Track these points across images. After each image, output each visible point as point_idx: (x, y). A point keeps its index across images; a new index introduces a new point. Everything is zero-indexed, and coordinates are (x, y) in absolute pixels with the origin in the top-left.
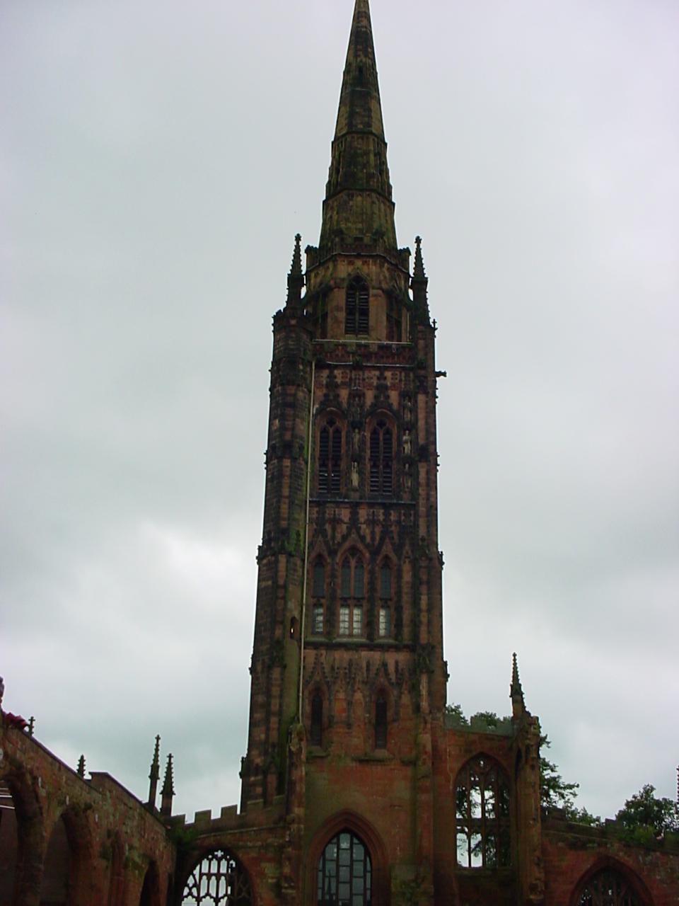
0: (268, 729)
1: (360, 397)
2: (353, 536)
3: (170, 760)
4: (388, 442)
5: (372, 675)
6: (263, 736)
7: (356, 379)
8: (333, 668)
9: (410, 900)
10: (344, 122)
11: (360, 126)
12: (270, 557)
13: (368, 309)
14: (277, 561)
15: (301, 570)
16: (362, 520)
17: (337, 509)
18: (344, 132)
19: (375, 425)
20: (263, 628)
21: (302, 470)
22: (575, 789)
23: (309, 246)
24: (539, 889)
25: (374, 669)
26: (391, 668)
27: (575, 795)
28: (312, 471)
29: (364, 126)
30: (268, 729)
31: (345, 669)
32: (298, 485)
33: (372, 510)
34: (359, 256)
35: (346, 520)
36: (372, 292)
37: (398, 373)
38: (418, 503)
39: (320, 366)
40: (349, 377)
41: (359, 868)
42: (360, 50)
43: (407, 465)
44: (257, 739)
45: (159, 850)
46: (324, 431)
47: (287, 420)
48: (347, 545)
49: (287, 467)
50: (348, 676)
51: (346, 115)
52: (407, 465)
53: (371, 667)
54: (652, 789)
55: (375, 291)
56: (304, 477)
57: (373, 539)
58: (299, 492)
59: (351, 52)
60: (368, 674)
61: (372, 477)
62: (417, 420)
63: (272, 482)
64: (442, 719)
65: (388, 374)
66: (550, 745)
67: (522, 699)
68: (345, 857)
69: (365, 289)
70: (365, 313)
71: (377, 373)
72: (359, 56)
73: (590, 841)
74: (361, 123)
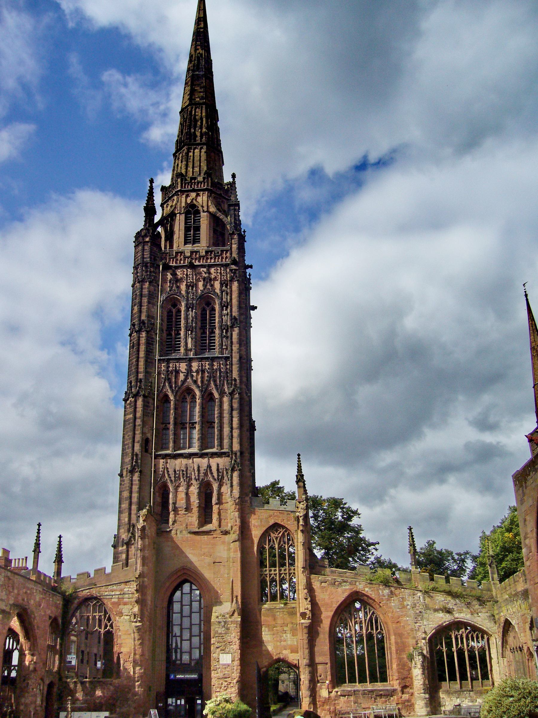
0: (130, 514)
1: (193, 287)
2: (188, 380)
3: (60, 539)
4: (212, 316)
5: (202, 474)
6: (127, 519)
7: (190, 274)
8: (175, 471)
9: (224, 626)
10: (187, 97)
11: (198, 99)
12: (131, 398)
13: (200, 226)
14: (136, 401)
15: (152, 406)
16: (194, 369)
17: (177, 364)
18: (187, 104)
19: (204, 305)
20: (127, 446)
21: (153, 338)
22: (377, 546)
23: (162, 186)
24: (307, 616)
25: (202, 471)
26: (214, 469)
27: (376, 550)
28: (161, 339)
29: (200, 99)
30: (130, 514)
31: (183, 471)
32: (151, 349)
33: (200, 363)
34: (194, 190)
35: (184, 370)
36: (202, 214)
37: (219, 269)
38: (232, 355)
39: (167, 267)
40: (185, 273)
41: (195, 605)
42: (198, 45)
43: (224, 331)
44: (123, 522)
45: (35, 600)
46: (170, 312)
47: (144, 306)
48: (183, 388)
49: (143, 337)
50: (185, 476)
51: (188, 93)
52: (224, 331)
53: (200, 469)
54: (434, 543)
55: (206, 214)
56: (155, 343)
57: (202, 382)
58: (150, 354)
59: (193, 47)
60: (199, 473)
61: (202, 340)
62: (231, 299)
63: (133, 348)
64: (249, 502)
65: (212, 270)
66: (360, 516)
67: (304, 484)
68: (186, 599)
69: (198, 212)
70: (197, 229)
71: (205, 270)
72: (198, 49)
73: (345, 582)
74: (198, 97)
